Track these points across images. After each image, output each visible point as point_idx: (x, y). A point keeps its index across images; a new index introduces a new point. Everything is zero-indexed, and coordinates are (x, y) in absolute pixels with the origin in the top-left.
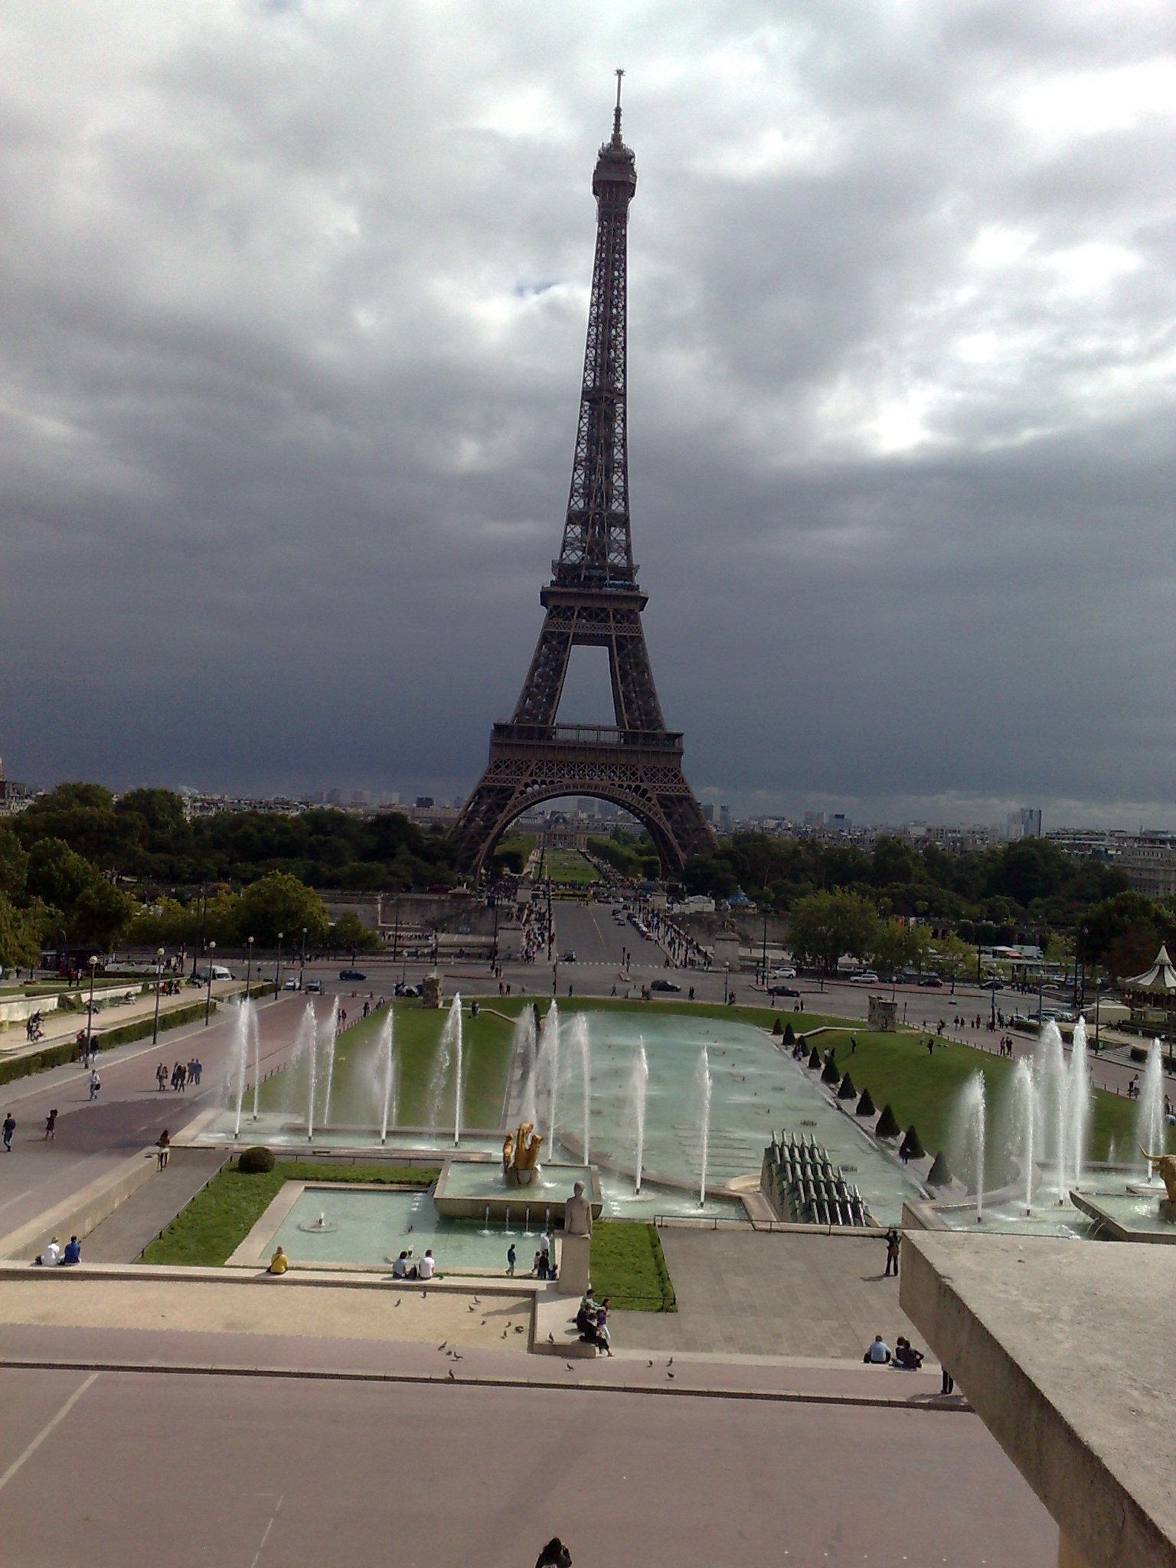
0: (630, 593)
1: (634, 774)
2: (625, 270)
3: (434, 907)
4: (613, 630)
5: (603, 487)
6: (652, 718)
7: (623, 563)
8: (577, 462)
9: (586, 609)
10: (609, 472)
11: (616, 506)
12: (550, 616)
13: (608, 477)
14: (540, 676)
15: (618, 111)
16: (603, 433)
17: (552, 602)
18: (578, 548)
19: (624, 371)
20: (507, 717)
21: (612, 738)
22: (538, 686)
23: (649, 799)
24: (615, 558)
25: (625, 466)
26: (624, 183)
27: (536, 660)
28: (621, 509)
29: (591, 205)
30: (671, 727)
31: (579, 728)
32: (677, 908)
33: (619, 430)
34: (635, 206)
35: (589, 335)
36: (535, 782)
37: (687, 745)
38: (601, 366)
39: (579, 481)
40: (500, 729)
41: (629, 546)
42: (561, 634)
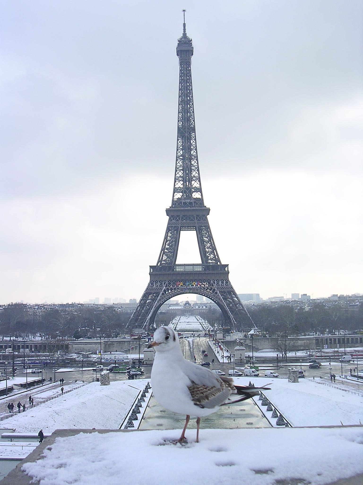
0: (203, 208)
1: (209, 283)
2: (191, 83)
3: (126, 344)
10: (190, 159)
11: (194, 173)
12: (170, 220)
13: (191, 162)
15: (184, 24)
16: (187, 145)
19: (194, 121)
20: (155, 264)
21: (200, 269)
22: (167, 249)
23: (216, 293)
24: (196, 195)
26: (188, 51)
27: (166, 238)
28: (197, 175)
30: (223, 263)
31: (185, 265)
32: (228, 338)
33: (194, 143)
35: (179, 108)
36: (168, 290)
37: (230, 269)
39: (179, 164)
40: (151, 267)
42: (175, 227)
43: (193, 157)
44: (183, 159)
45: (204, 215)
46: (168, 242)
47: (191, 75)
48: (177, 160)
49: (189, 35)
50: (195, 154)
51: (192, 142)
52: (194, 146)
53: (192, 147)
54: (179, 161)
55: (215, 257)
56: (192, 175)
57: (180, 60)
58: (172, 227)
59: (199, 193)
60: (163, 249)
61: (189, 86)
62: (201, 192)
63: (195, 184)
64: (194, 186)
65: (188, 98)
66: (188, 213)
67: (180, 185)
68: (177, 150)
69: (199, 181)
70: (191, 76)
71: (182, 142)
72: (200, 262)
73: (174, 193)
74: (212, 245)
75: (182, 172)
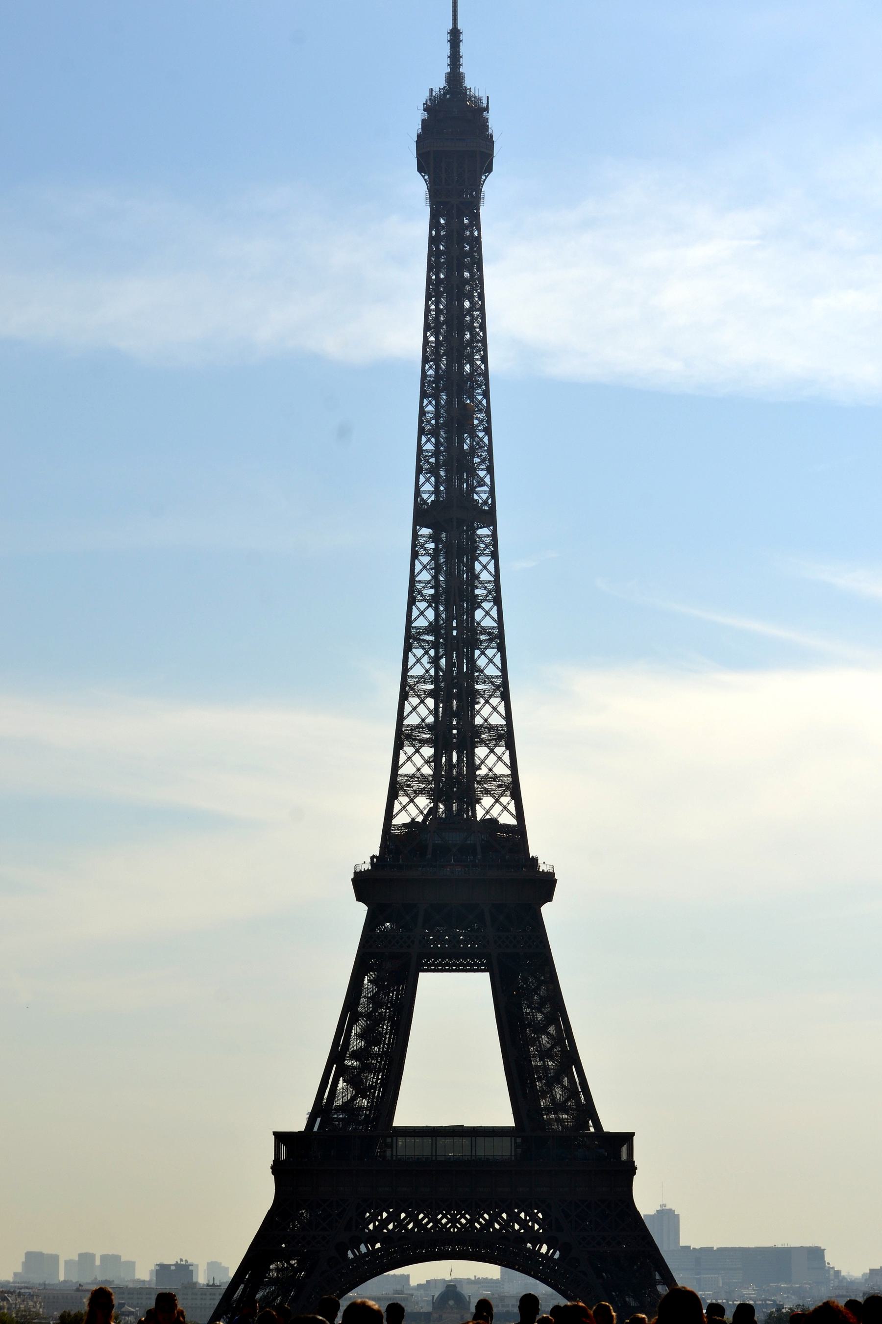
2: (481, 297)
7: (507, 819)
8: (411, 638)
11: (488, 713)
15: (455, 37)
18: (420, 792)
19: (490, 470)
20: (298, 1124)
21: (504, 1149)
22: (355, 1055)
25: (501, 636)
29: (416, 189)
30: (611, 1123)
34: (495, 191)
35: (422, 413)
37: (642, 1155)
38: (447, 464)
43: (483, 637)
44: (435, 645)
46: (362, 1022)
47: (479, 264)
48: (408, 648)
49: (475, 82)
50: (488, 623)
51: (478, 567)
52: (490, 586)
53: (477, 592)
54: (419, 652)
56: (478, 721)
59: (505, 800)
60: (336, 1056)
61: (470, 311)
62: (516, 795)
63: (490, 761)
64: (483, 771)
65: (467, 368)
67: (418, 762)
68: (412, 602)
69: (511, 747)
70: (480, 269)
71: (437, 569)
73: (393, 796)
75: (430, 702)
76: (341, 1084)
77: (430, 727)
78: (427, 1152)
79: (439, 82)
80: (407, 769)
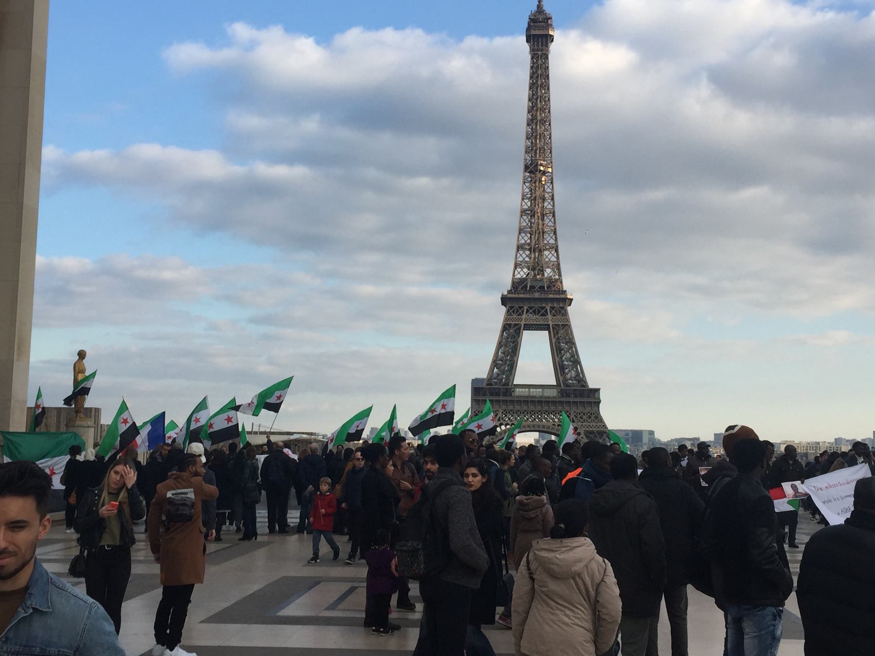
0: (562, 296)
2: (548, 89)
4: (550, 319)
5: (540, 227)
6: (581, 380)
8: (523, 212)
9: (531, 308)
13: (543, 220)
14: (504, 353)
17: (509, 305)
21: (553, 393)
28: (552, 241)
30: (592, 385)
36: (501, 425)
41: (559, 264)
42: (516, 325)
45: (562, 308)
47: (548, 76)
49: (548, 8)
55: (578, 375)
57: (532, 50)
58: (510, 325)
66: (536, 302)
69: (557, 251)
72: (553, 382)
74: (573, 356)
75: (529, 235)
76: (496, 370)
77: (529, 244)
78: (527, 394)
79: (535, 8)
80: (520, 259)
